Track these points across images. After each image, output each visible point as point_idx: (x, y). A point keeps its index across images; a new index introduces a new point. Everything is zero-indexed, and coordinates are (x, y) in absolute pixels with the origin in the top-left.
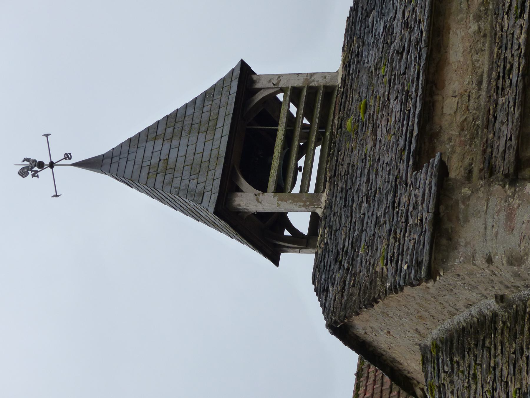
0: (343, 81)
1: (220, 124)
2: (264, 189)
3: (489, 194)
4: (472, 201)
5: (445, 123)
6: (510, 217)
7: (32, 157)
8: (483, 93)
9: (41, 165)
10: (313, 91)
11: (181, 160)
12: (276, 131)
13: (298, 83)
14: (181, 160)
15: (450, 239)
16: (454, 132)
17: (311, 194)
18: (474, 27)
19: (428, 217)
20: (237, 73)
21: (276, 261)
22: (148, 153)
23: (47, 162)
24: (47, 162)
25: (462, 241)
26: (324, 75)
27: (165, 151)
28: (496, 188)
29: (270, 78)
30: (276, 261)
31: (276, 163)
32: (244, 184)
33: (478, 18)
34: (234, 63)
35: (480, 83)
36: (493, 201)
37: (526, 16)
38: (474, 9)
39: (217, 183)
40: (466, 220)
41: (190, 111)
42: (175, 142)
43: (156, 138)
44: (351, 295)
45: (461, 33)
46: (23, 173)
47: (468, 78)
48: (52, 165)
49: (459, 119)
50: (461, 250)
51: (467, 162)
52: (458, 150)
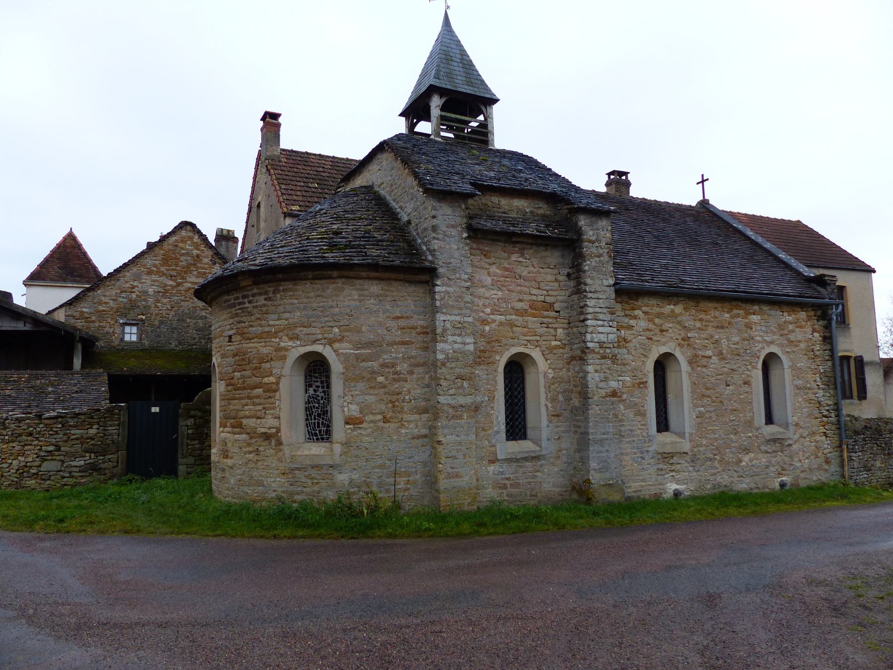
0: (491, 149)
3: (462, 217)
4: (459, 209)
5: (487, 197)
6: (453, 226)
8: (500, 214)
10: (486, 134)
12: (467, 116)
13: (489, 128)
14: (453, 68)
15: (442, 199)
18: (528, 210)
21: (401, 115)
22: (454, 51)
26: (493, 140)
28: (465, 220)
29: (491, 114)
30: (401, 115)
31: (453, 116)
32: (443, 100)
33: (531, 212)
34: (498, 96)
35: (504, 213)
36: (459, 219)
37: (538, 233)
38: (535, 210)
39: (444, 86)
40: (451, 207)
42: (460, 65)
45: (525, 204)
49: (489, 203)
50: (438, 204)
52: (476, 203)
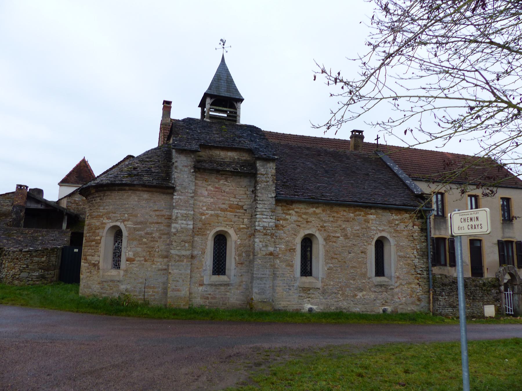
0: (237, 125)
1: (228, 94)
2: (211, 105)
3: (192, 162)
4: (190, 158)
5: (213, 151)
6: (186, 166)
7: (226, 42)
8: (219, 160)
9: (224, 45)
10: (236, 117)
11: (220, 83)
12: (227, 108)
13: (238, 113)
14: (220, 83)
15: (181, 153)
16: (211, 153)
17: (189, 121)
18: (236, 158)
19: (186, 148)
20: (241, 98)
21: (199, 107)
22: (223, 74)
23: (224, 46)
24: (224, 46)
25: (181, 156)
26: (239, 120)
27: (223, 79)
28: (193, 163)
29: (240, 106)
30: (199, 107)
32: (212, 100)
33: (238, 158)
34: (244, 97)
35: (222, 159)
36: (190, 163)
37: (233, 170)
38: (240, 158)
39: (213, 93)
40: (186, 157)
41: (233, 85)
42: (225, 82)
43: (227, 76)
44: (177, 128)
45: (235, 155)
46: (222, 40)
47: (223, 156)
48: (223, 48)
49: (214, 154)
50: (179, 155)
51: (203, 156)
52: (206, 154)
